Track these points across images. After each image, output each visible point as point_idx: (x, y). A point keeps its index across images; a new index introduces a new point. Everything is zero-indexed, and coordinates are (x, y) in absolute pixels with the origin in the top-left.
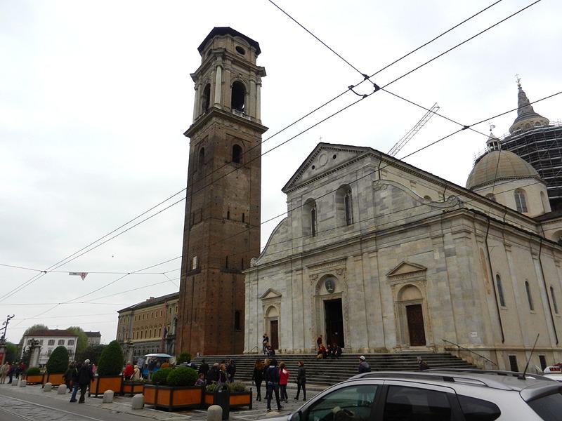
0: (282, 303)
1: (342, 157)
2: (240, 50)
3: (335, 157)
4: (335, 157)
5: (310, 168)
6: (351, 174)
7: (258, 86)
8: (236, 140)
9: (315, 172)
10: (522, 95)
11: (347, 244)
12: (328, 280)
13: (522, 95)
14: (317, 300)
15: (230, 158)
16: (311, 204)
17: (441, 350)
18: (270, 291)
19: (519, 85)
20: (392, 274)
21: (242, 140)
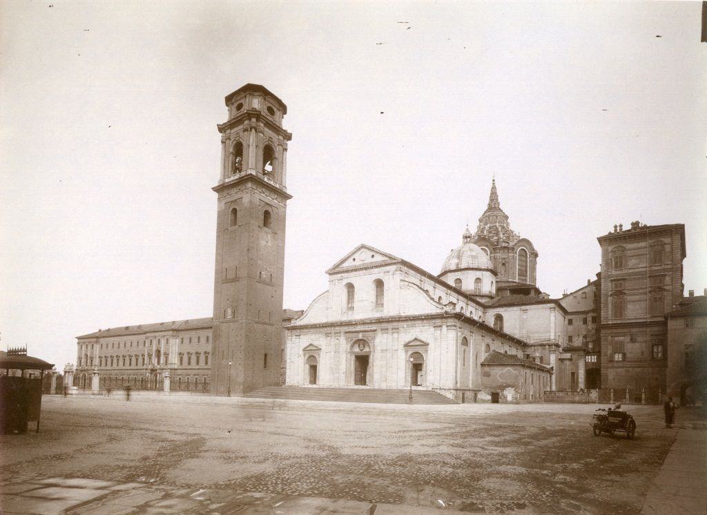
0: (321, 355)
1: (378, 258)
2: (270, 110)
3: (373, 256)
4: (373, 256)
5: (351, 259)
6: (385, 273)
7: (285, 152)
8: (267, 206)
9: (354, 263)
10: (494, 188)
11: (380, 321)
12: (362, 342)
13: (494, 188)
14: (351, 355)
15: (262, 224)
16: (350, 287)
17: (430, 389)
18: (311, 345)
19: (494, 181)
20: (407, 345)
21: (271, 206)
